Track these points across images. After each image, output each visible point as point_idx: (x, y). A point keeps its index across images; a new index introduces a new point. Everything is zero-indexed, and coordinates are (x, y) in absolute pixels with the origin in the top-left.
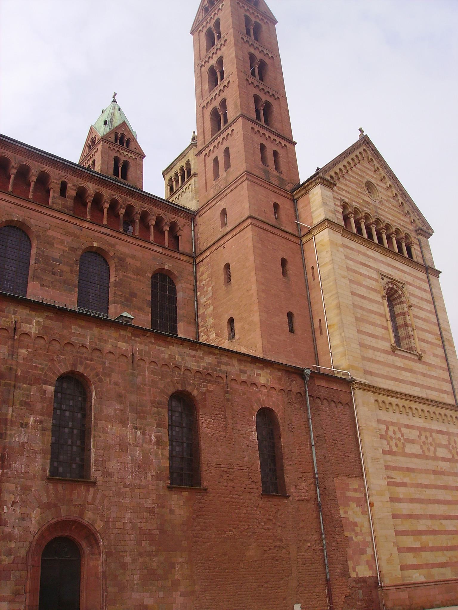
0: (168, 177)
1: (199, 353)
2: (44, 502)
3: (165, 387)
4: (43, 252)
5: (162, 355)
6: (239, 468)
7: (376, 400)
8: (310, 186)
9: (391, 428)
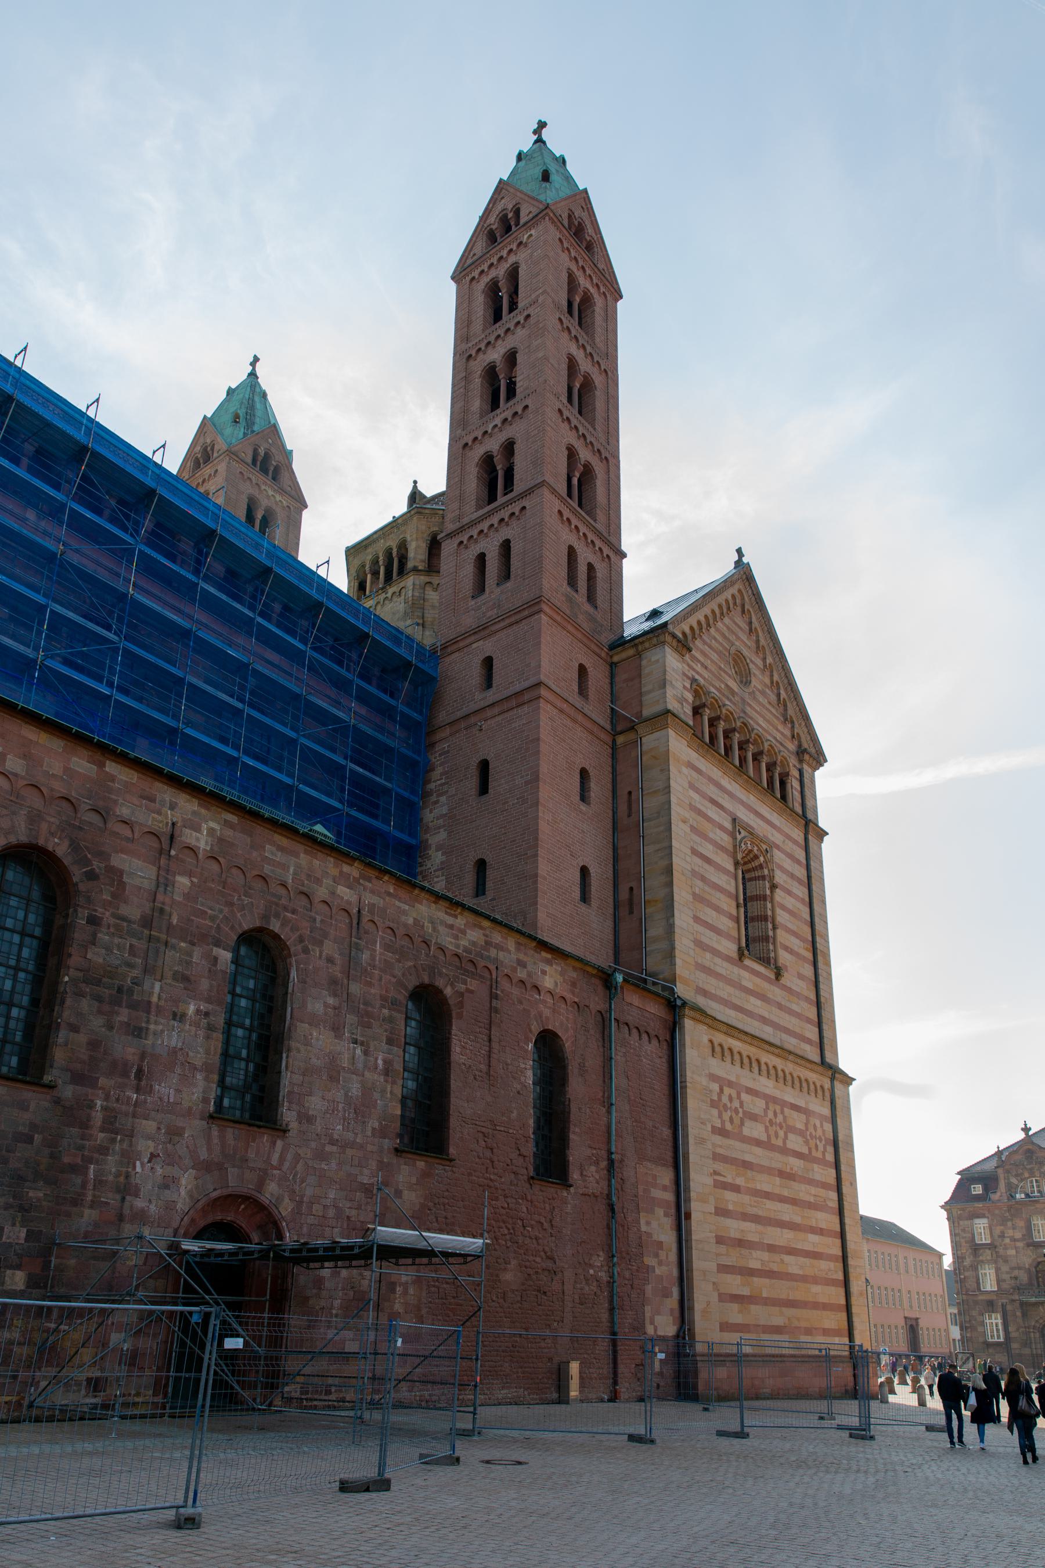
0: (357, 562)
1: (460, 921)
2: (202, 1158)
3: (404, 975)
5: (403, 918)
6: (502, 1129)
7: (711, 1041)
8: (647, 645)
9: (727, 1091)
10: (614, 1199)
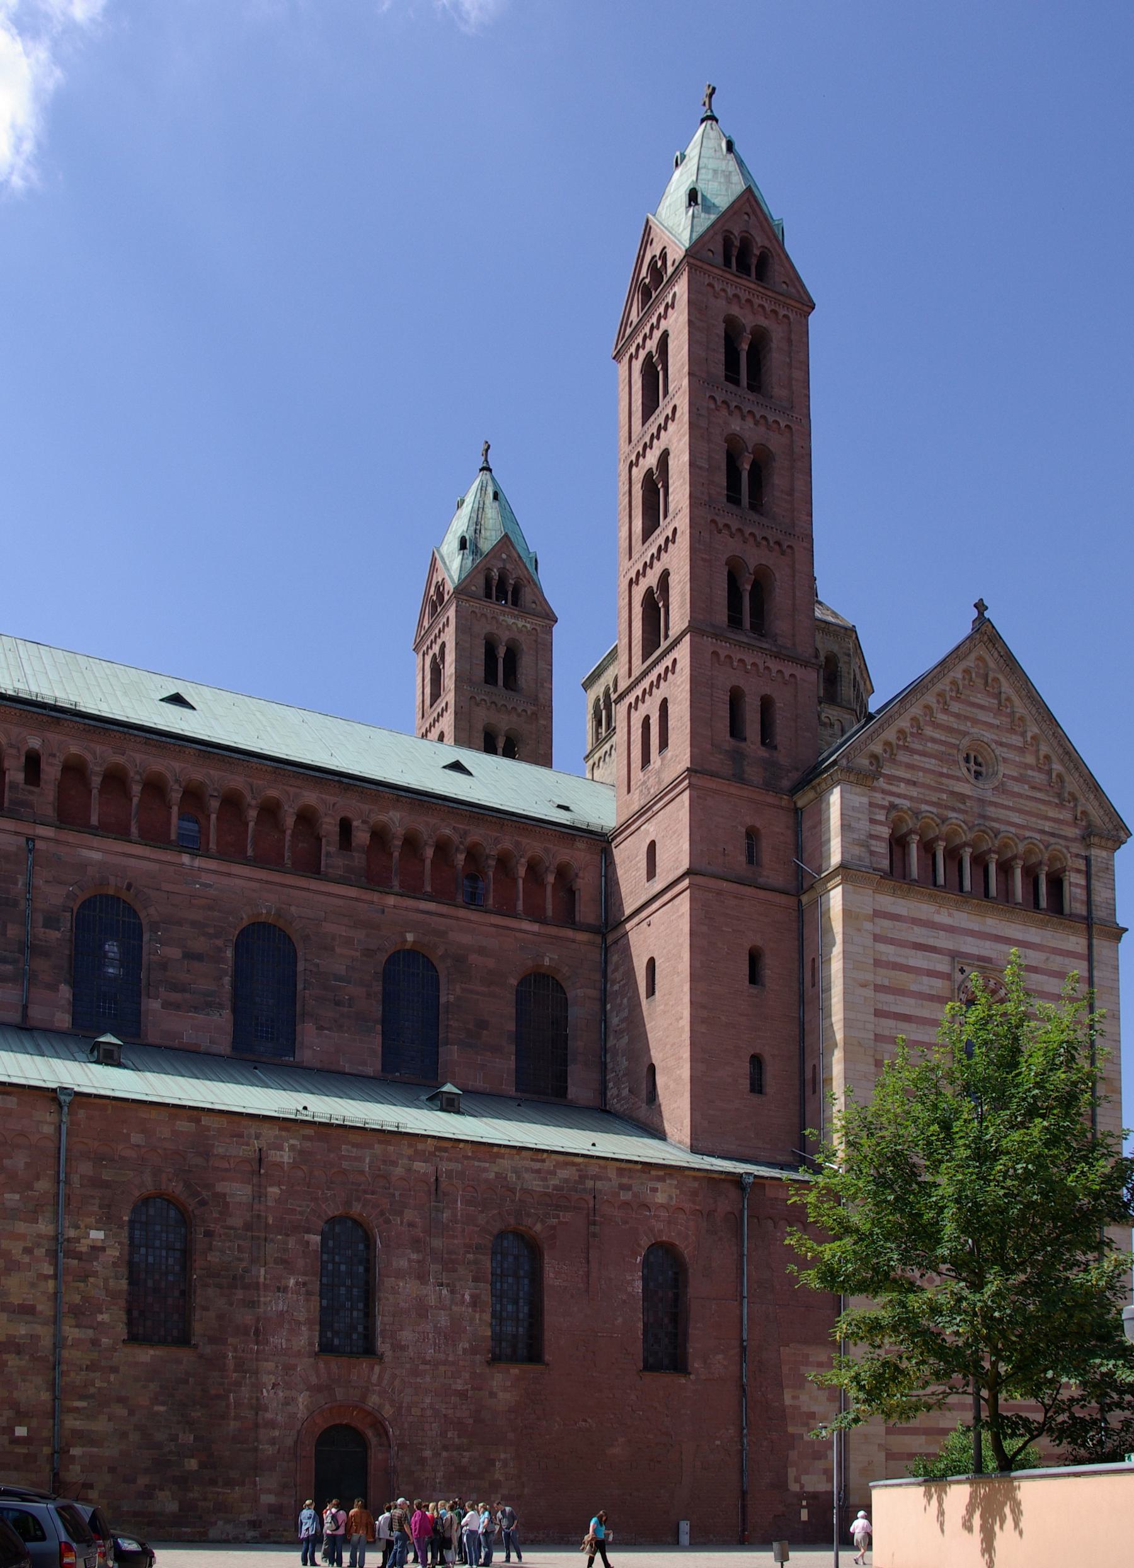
4: (318, 965)
5: (484, 1175)
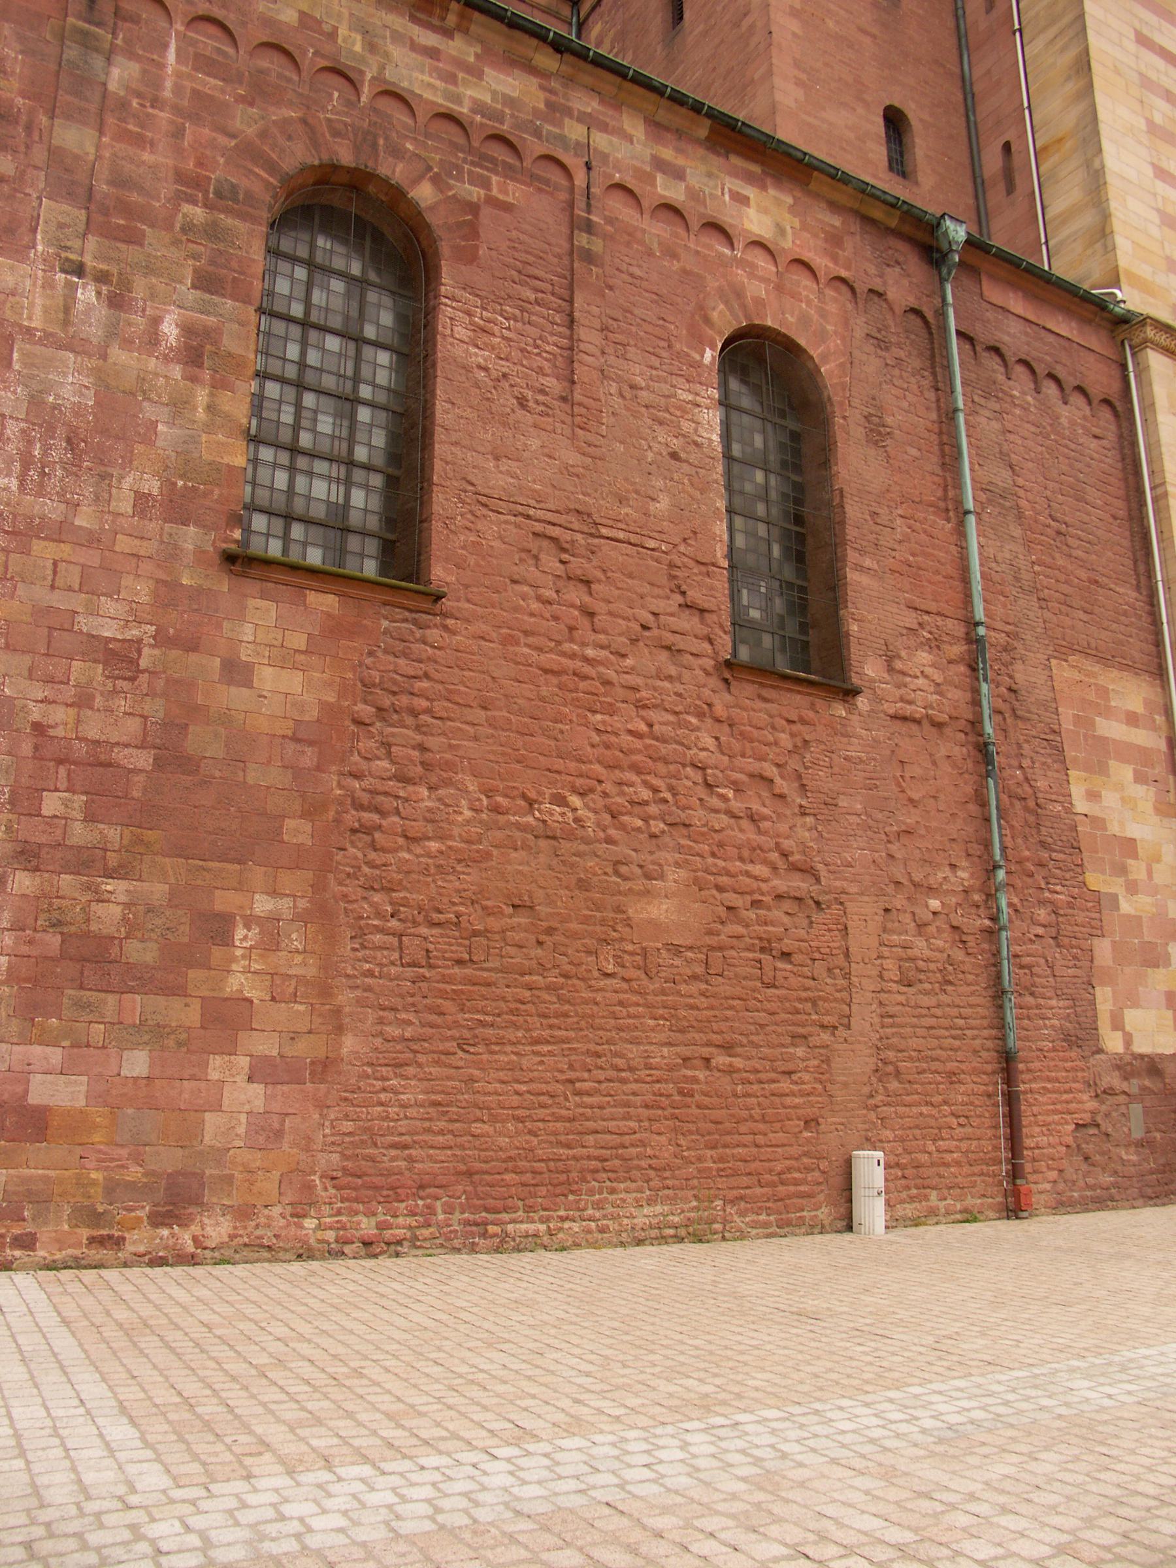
3: (264, 134)
6: (621, 535)
10: (989, 729)
